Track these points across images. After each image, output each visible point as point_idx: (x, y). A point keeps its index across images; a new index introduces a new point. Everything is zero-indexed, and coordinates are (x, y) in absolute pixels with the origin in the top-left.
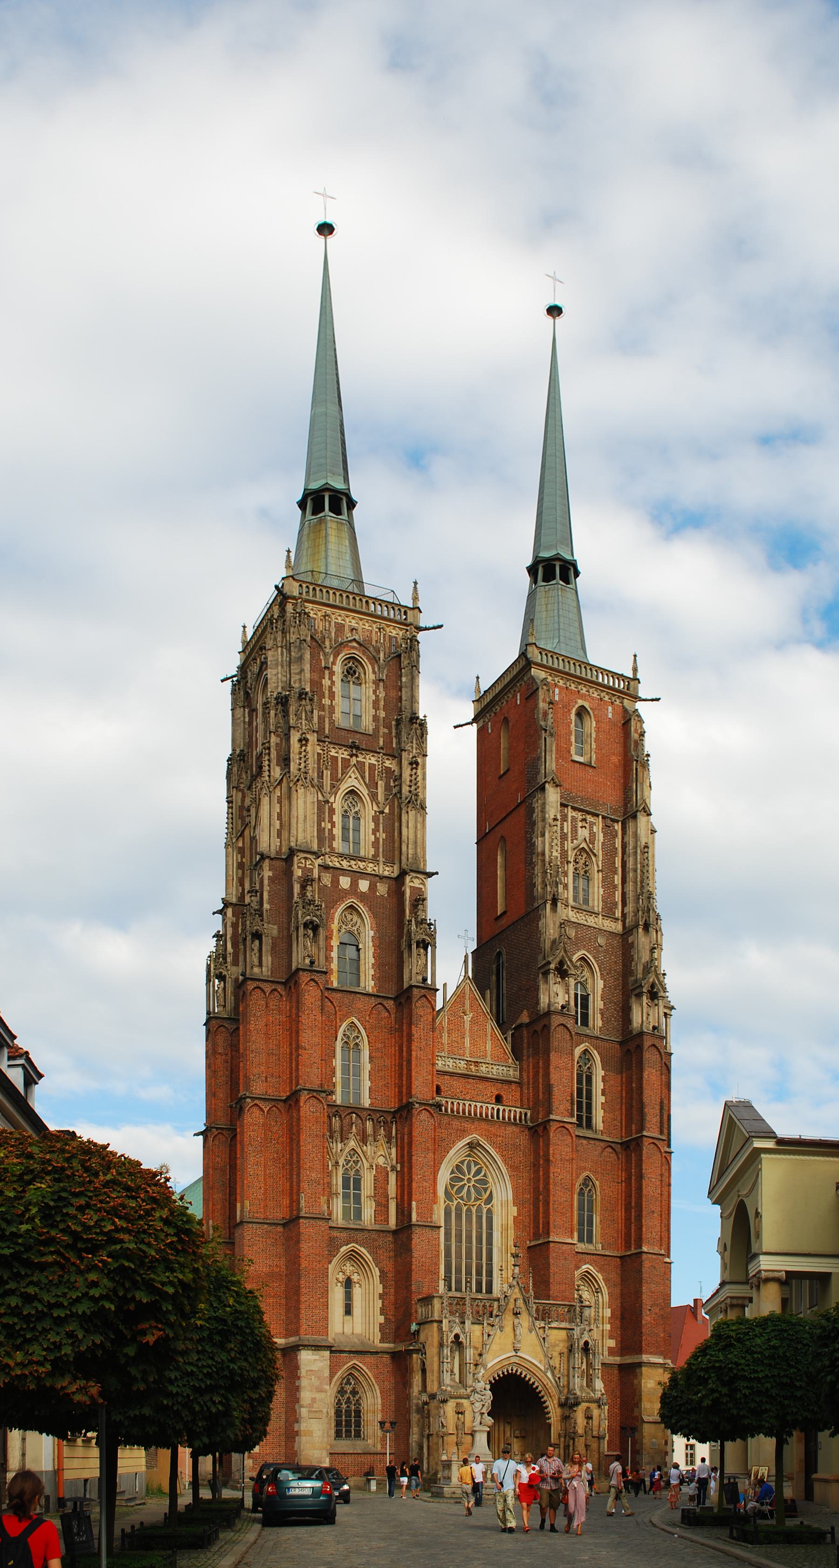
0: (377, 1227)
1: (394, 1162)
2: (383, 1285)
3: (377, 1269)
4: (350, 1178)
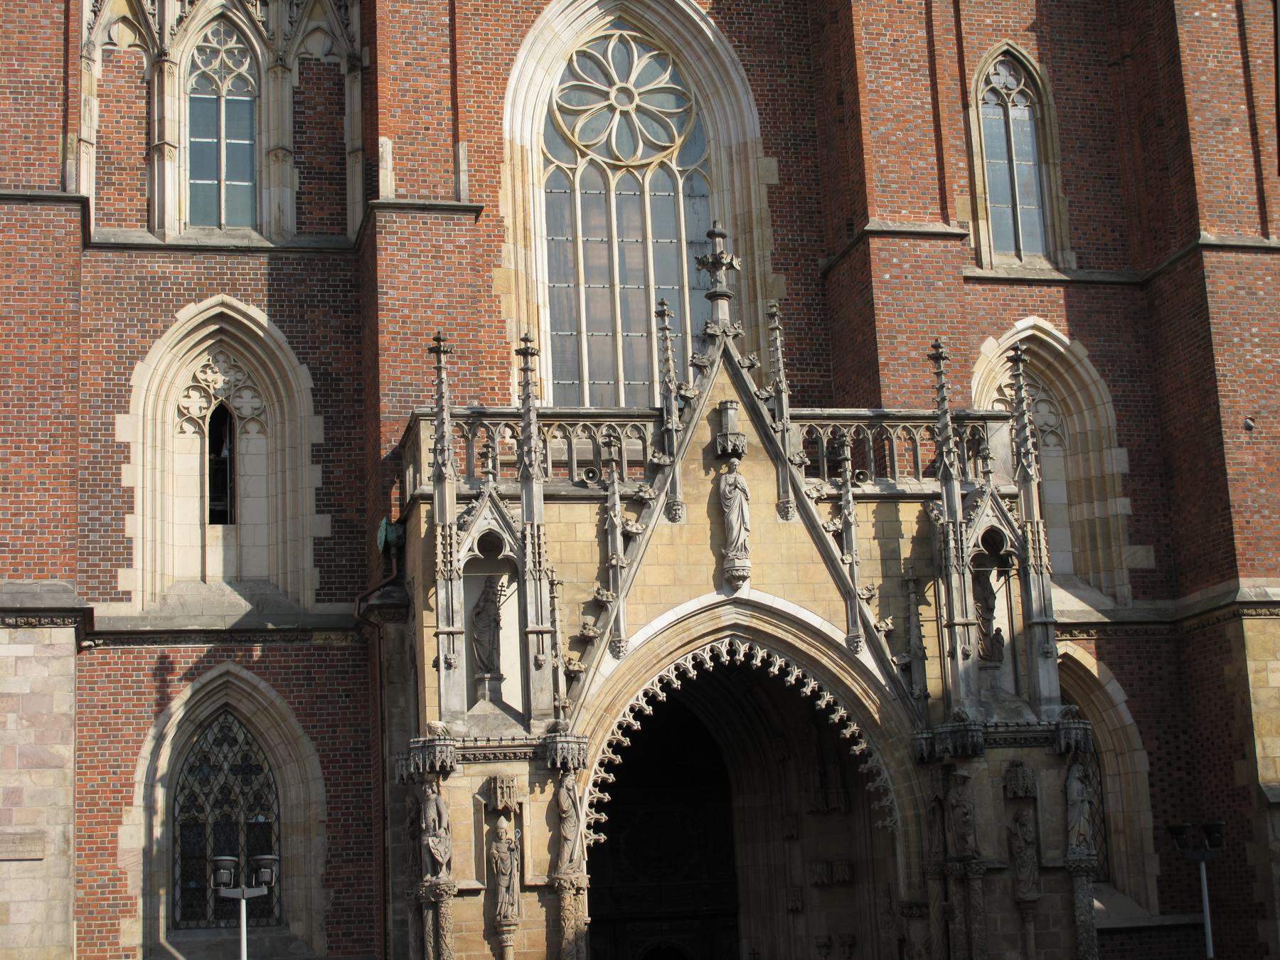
0: (305, 241)
1: (357, 45)
2: (327, 420)
3: (304, 371)
4: (218, 99)
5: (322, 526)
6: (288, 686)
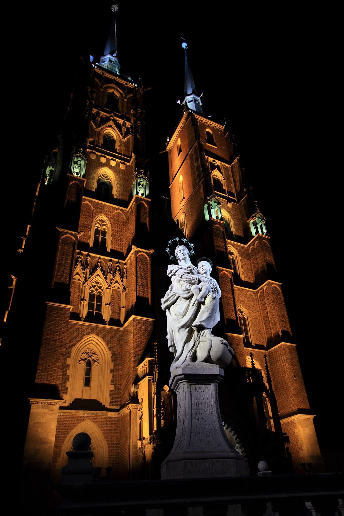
5: (112, 388)
6: (101, 426)
